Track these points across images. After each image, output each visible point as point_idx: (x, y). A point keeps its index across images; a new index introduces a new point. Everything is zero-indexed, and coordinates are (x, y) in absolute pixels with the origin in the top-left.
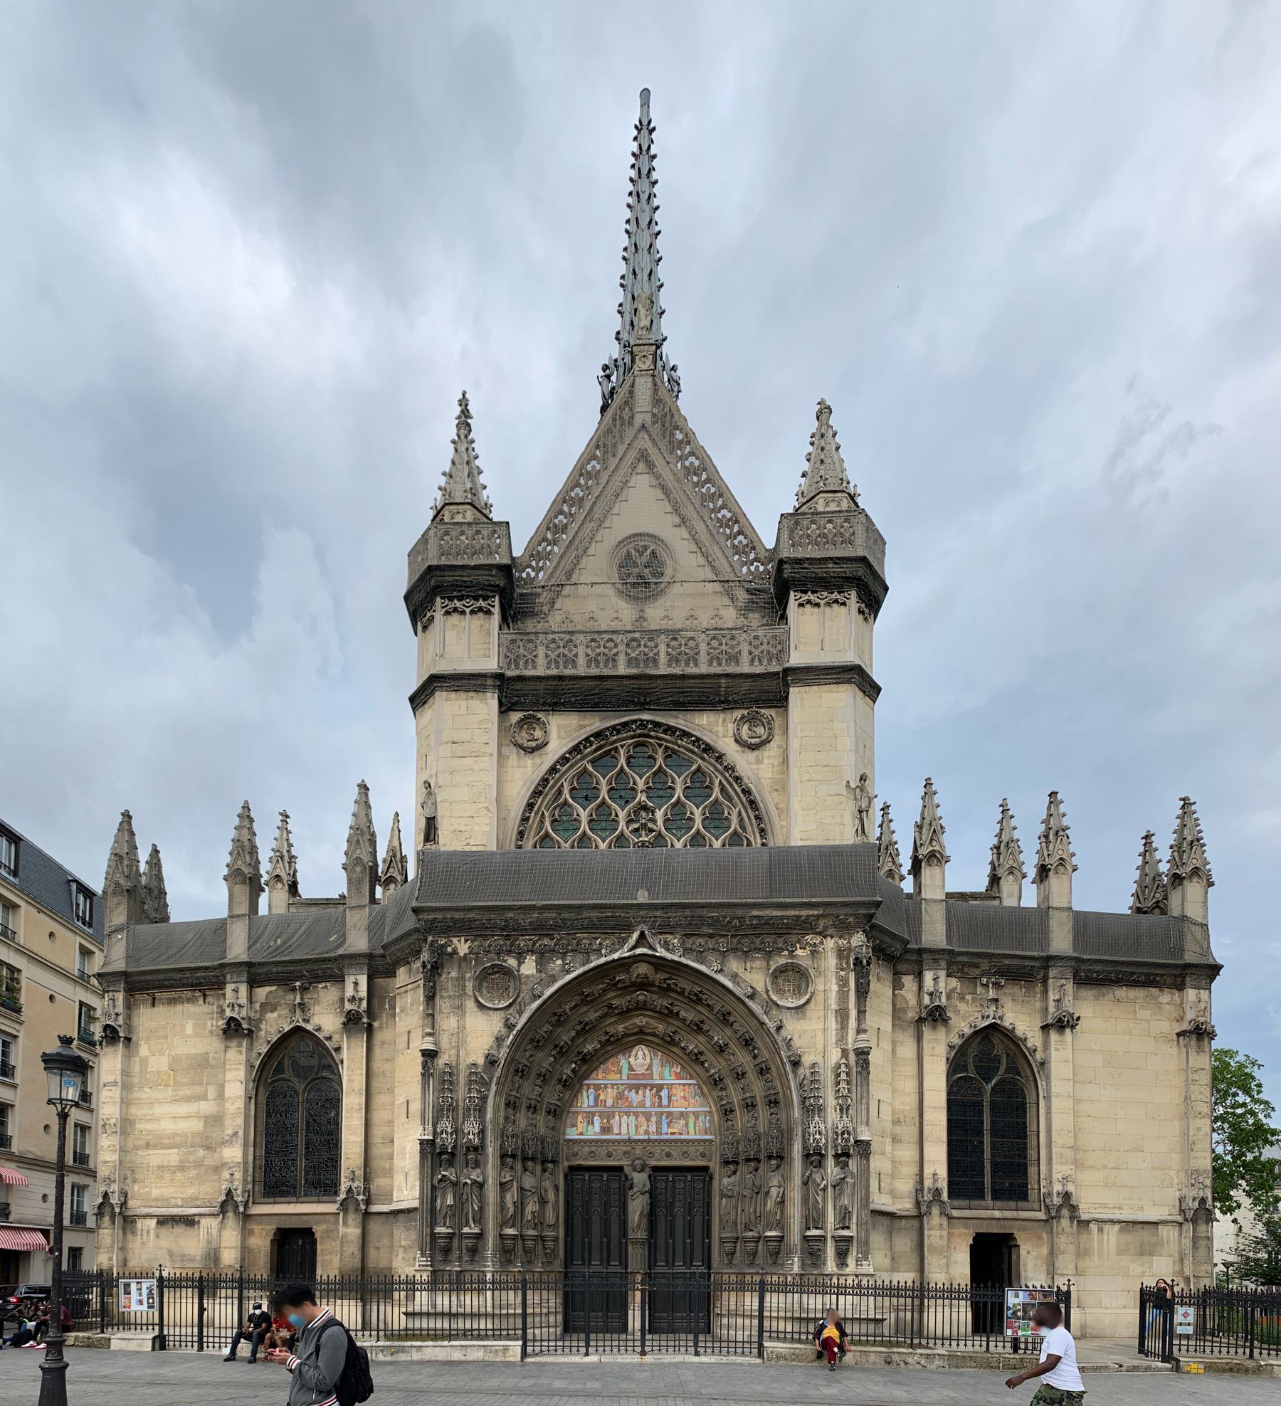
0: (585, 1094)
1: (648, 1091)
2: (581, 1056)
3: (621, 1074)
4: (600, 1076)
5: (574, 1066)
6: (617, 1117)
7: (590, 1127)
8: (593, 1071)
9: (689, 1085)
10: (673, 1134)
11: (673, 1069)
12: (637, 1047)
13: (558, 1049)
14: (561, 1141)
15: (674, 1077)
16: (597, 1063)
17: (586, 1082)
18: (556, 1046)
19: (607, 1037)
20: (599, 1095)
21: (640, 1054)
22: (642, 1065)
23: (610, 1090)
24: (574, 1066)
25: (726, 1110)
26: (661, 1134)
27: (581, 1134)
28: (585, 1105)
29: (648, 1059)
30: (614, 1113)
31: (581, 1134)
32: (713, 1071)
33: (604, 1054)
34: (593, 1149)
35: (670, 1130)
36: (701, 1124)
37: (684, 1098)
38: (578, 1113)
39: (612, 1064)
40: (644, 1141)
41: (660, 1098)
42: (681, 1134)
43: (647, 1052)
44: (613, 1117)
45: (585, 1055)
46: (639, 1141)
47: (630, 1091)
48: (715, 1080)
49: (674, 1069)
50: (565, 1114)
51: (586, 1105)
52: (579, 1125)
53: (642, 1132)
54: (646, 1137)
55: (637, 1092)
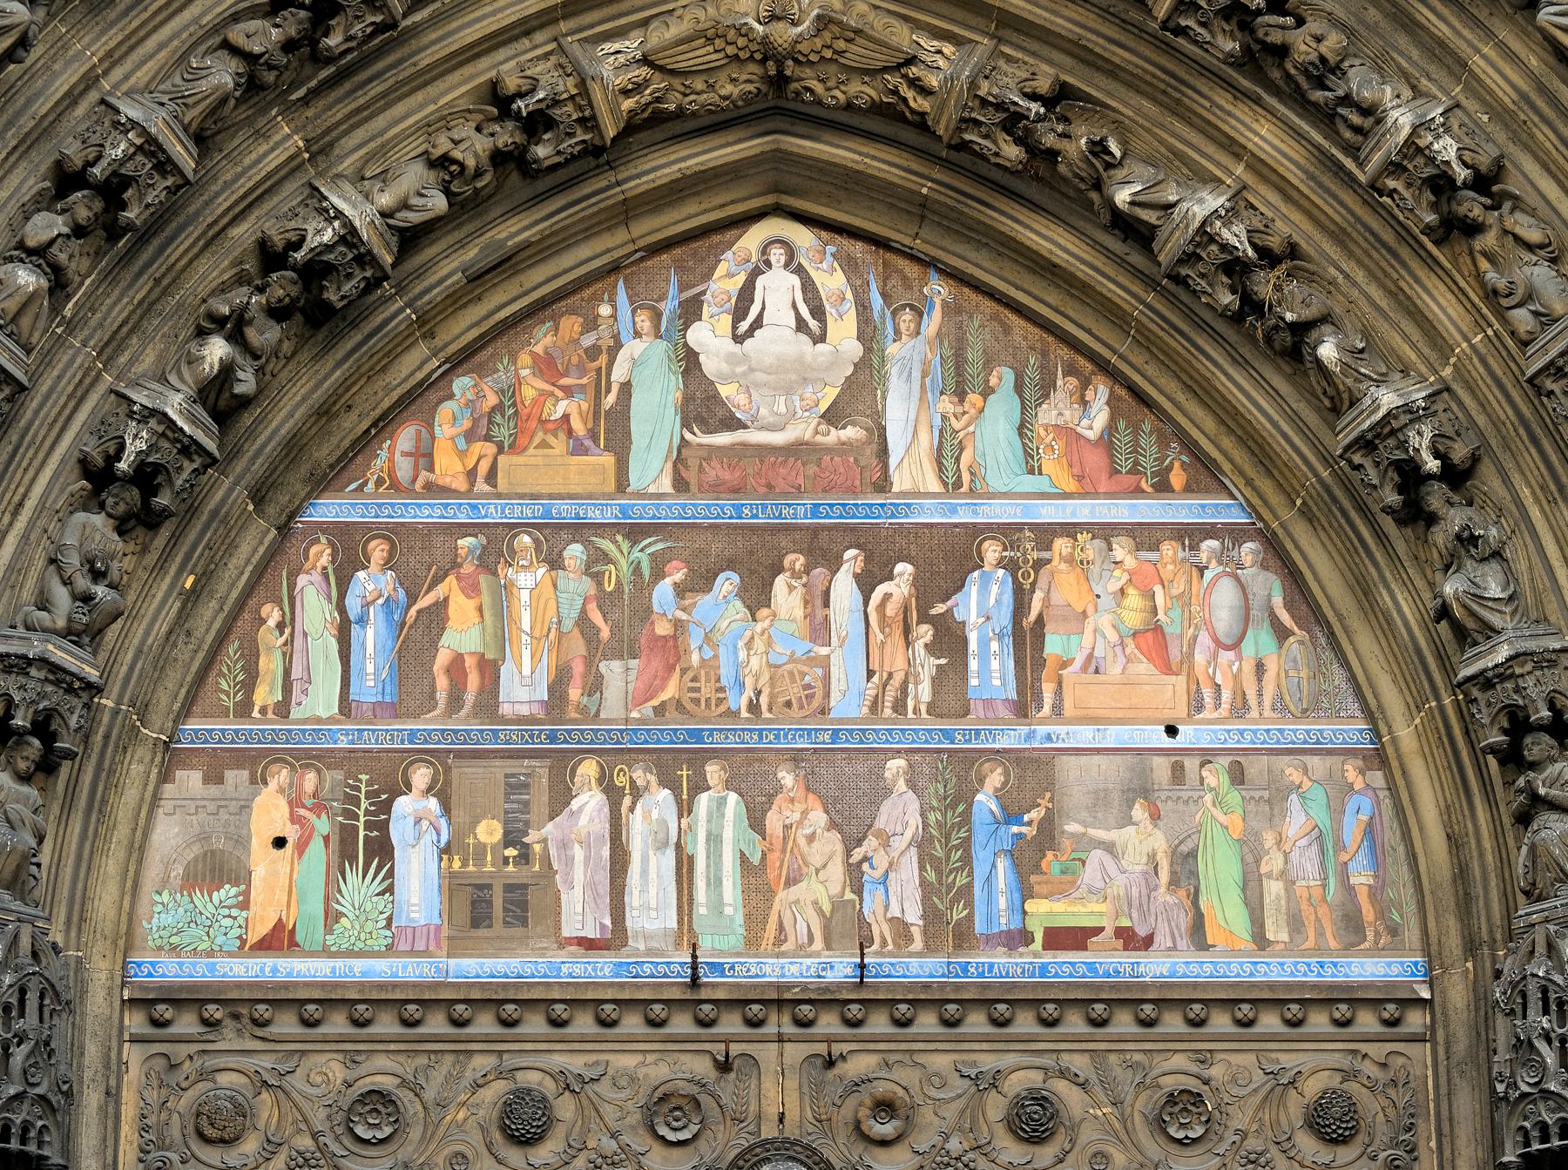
0: (315, 608)
1: (844, 587)
2: (282, 286)
3: (619, 443)
4: (448, 467)
5: (217, 350)
6: (589, 804)
7: (358, 888)
8: (384, 423)
9: (1191, 535)
10: (1061, 938)
11: (1047, 415)
12: (753, 238)
13: (83, 206)
14: (98, 1002)
15: (1055, 471)
16: (415, 362)
17: (328, 509)
18: (66, 180)
19: (506, 136)
20: (437, 616)
21: (778, 289)
22: (800, 377)
23: (527, 579)
24: (217, 350)
25: (1518, 724)
26: (963, 937)
27: (279, 940)
28: (320, 700)
29: (843, 331)
30: (562, 764)
31: (279, 940)
32: (1388, 399)
33: (479, 279)
34: (382, 1072)
35: (1044, 912)
36: (1307, 864)
37: (1152, 638)
38: (257, 763)
39: (547, 367)
40: (827, 1000)
41: (950, 640)
42: (1130, 939)
43: (831, 281)
44: (561, 798)
45: (316, 271)
46: (781, 1000)
47: (700, 581)
48: (1410, 476)
49: (1055, 411)
50: (137, 768)
51: (320, 700)
52: (264, 865)
53: (805, 923)
54: (841, 969)
55: (757, 596)
